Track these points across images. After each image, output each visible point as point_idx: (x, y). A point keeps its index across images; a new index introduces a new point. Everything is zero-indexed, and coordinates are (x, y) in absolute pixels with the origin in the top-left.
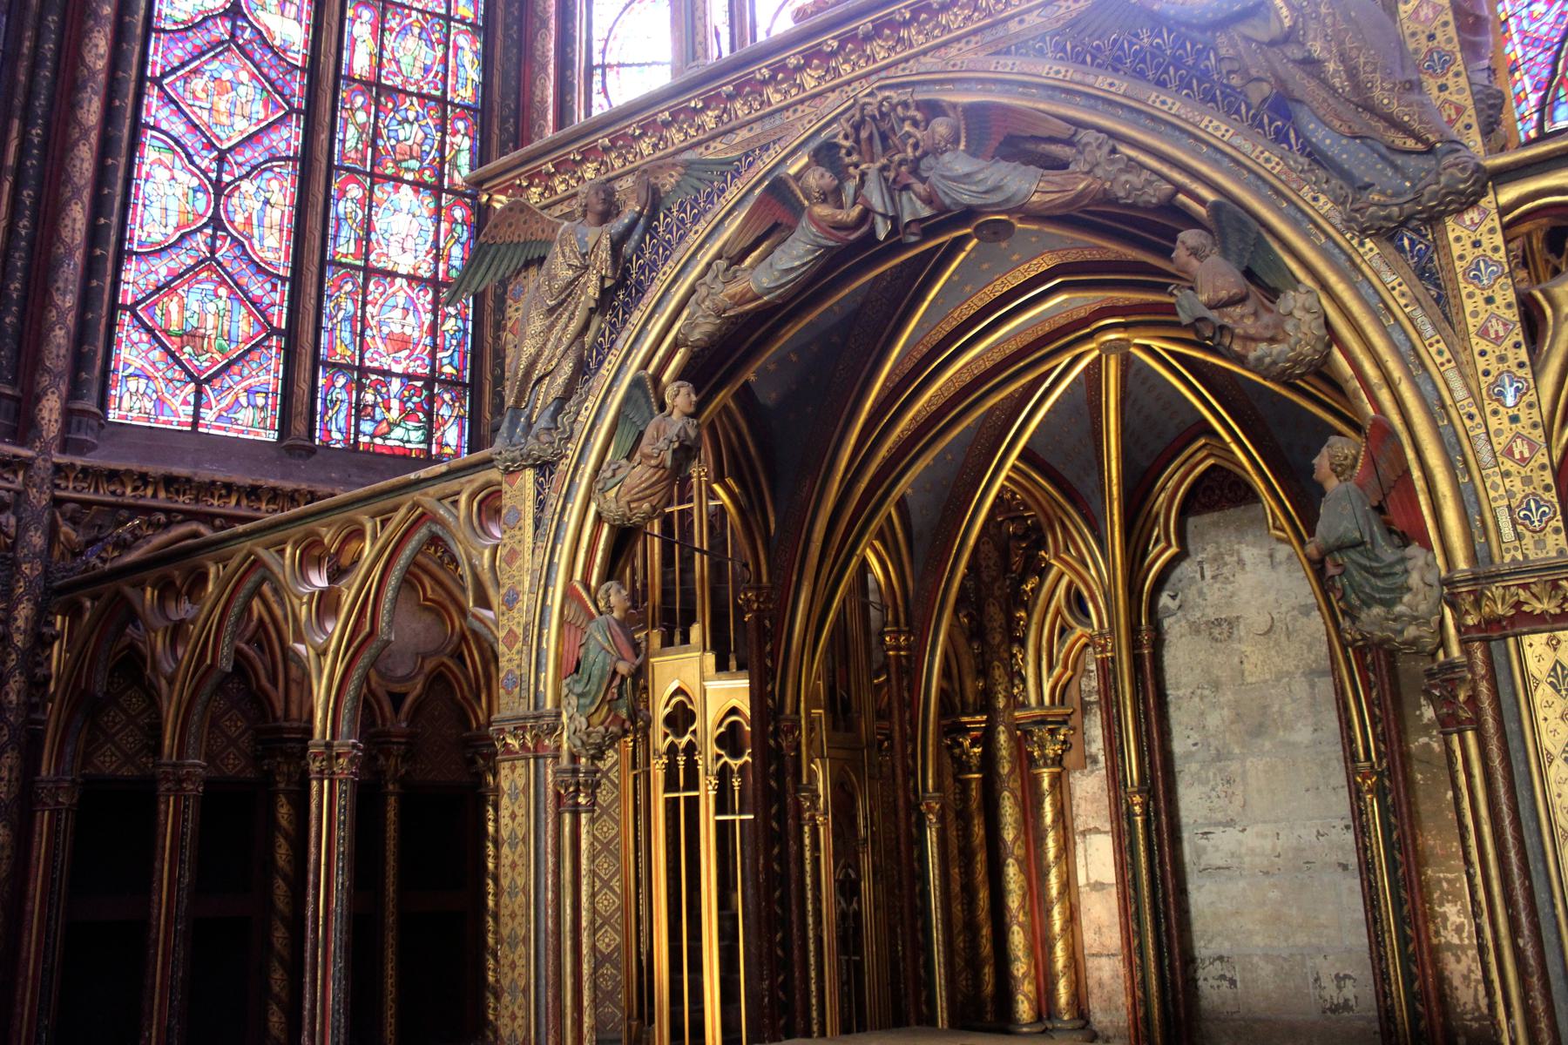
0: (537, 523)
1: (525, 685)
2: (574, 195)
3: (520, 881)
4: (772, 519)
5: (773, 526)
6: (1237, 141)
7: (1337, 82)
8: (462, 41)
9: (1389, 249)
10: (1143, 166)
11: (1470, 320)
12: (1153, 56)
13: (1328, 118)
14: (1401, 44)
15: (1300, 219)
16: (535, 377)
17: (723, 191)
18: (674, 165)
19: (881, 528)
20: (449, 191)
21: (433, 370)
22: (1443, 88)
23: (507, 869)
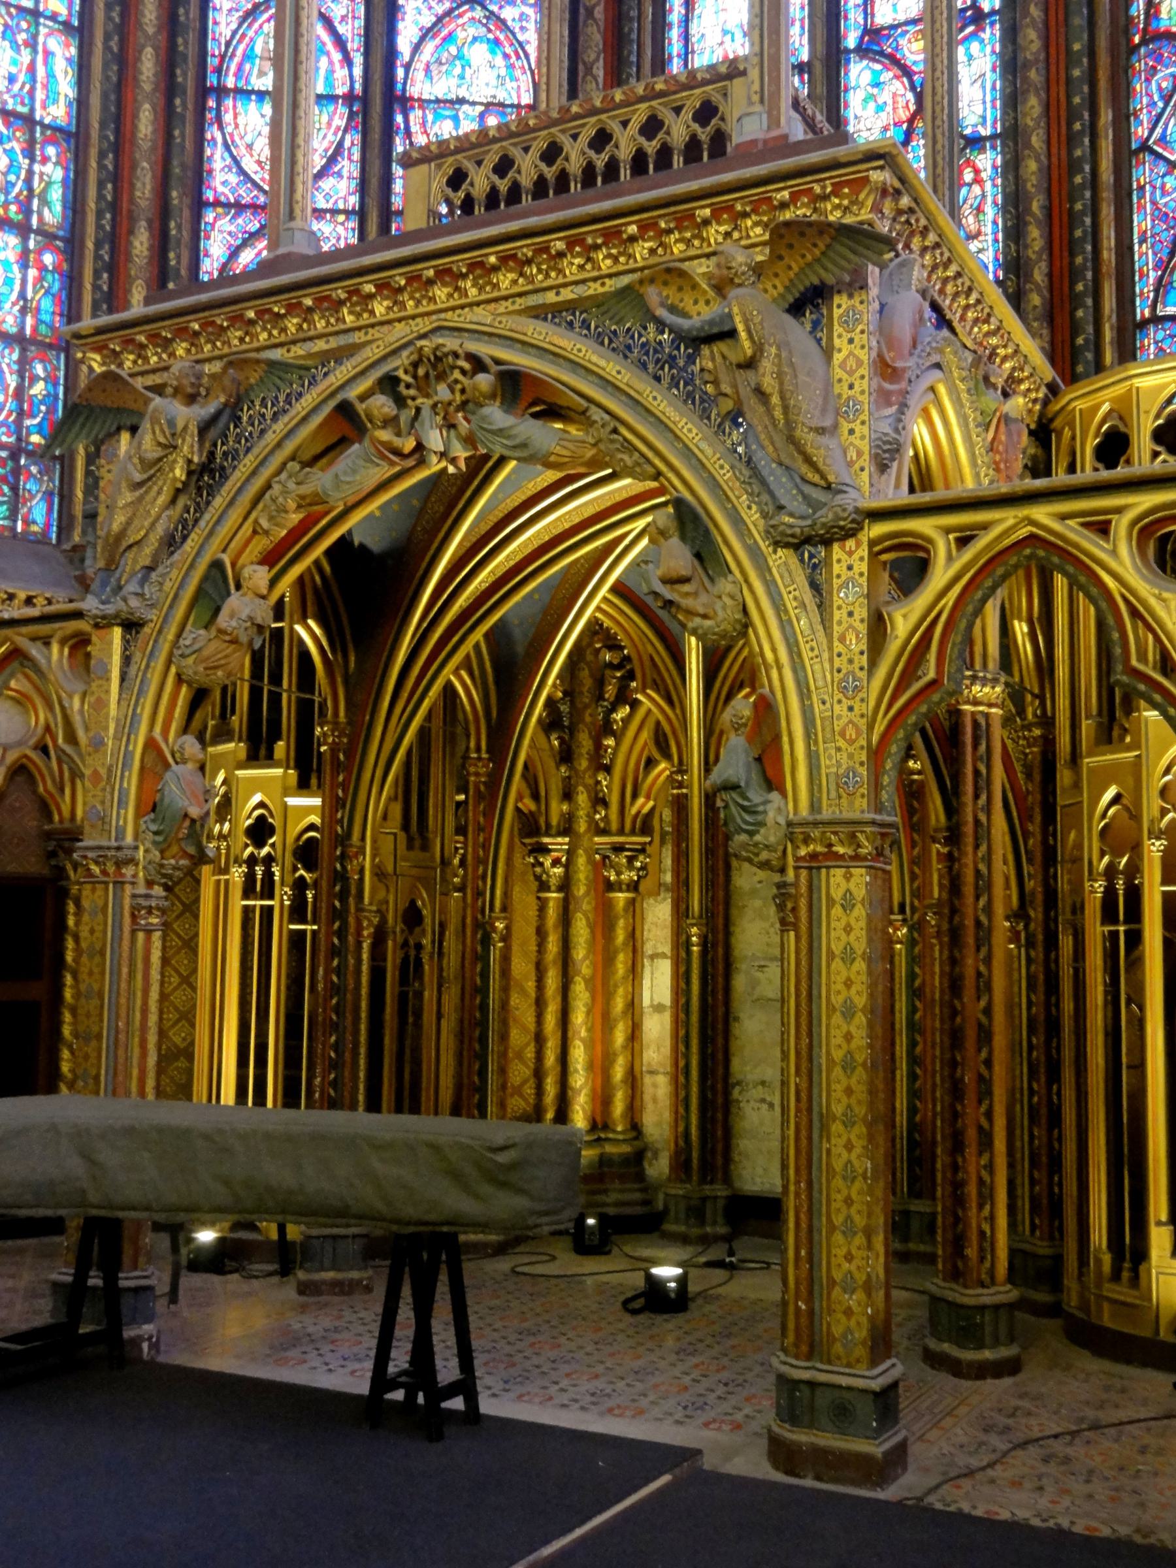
0: (123, 678)
2: (166, 369)
3: (96, 987)
4: (352, 659)
5: (352, 665)
7: (778, 413)
8: (55, 44)
10: (636, 449)
11: (835, 627)
12: (656, 351)
13: (766, 443)
14: (828, 385)
15: (737, 521)
16: (124, 544)
17: (300, 395)
18: (258, 361)
19: (468, 656)
20: (38, 232)
21: (19, 439)
22: (851, 432)
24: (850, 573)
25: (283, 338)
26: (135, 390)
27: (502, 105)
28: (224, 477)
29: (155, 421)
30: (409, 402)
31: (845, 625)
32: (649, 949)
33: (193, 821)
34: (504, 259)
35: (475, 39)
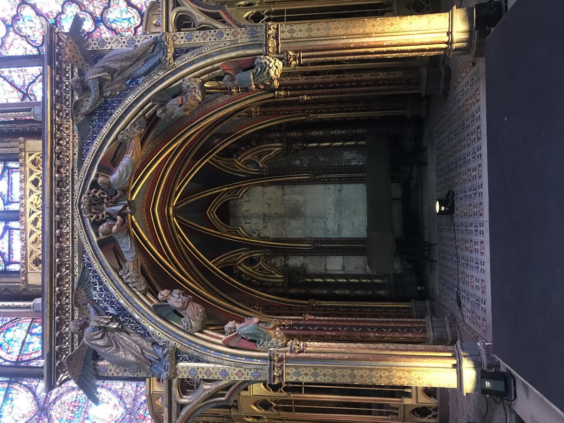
0: (198, 361)
1: (258, 367)
3: (331, 372)
6: (136, 94)
7: (129, 63)
9: (178, 59)
10: (134, 123)
13: (138, 67)
17: (94, 271)
18: (77, 289)
22: (139, 41)
23: (326, 378)
24: (184, 38)
25: (70, 277)
26: (78, 350)
27: (29, 328)
28: (122, 310)
29: (90, 339)
30: (105, 218)
31: (201, 38)
32: (324, 272)
33: (260, 322)
34: (59, 172)
35: (4, 337)
